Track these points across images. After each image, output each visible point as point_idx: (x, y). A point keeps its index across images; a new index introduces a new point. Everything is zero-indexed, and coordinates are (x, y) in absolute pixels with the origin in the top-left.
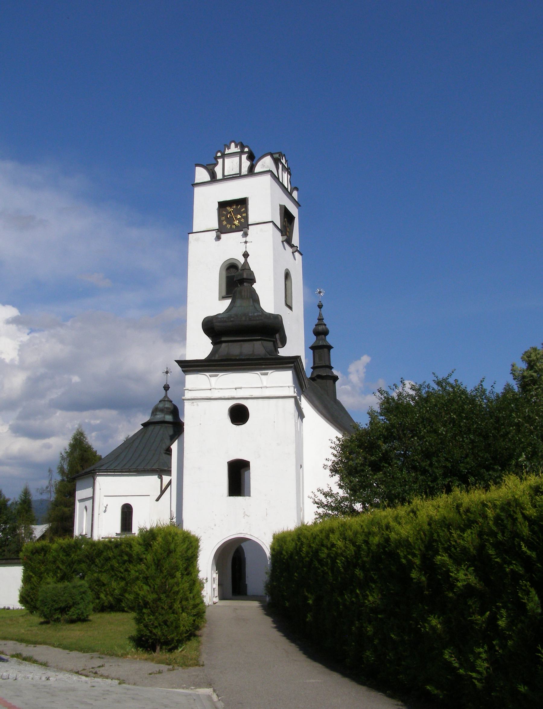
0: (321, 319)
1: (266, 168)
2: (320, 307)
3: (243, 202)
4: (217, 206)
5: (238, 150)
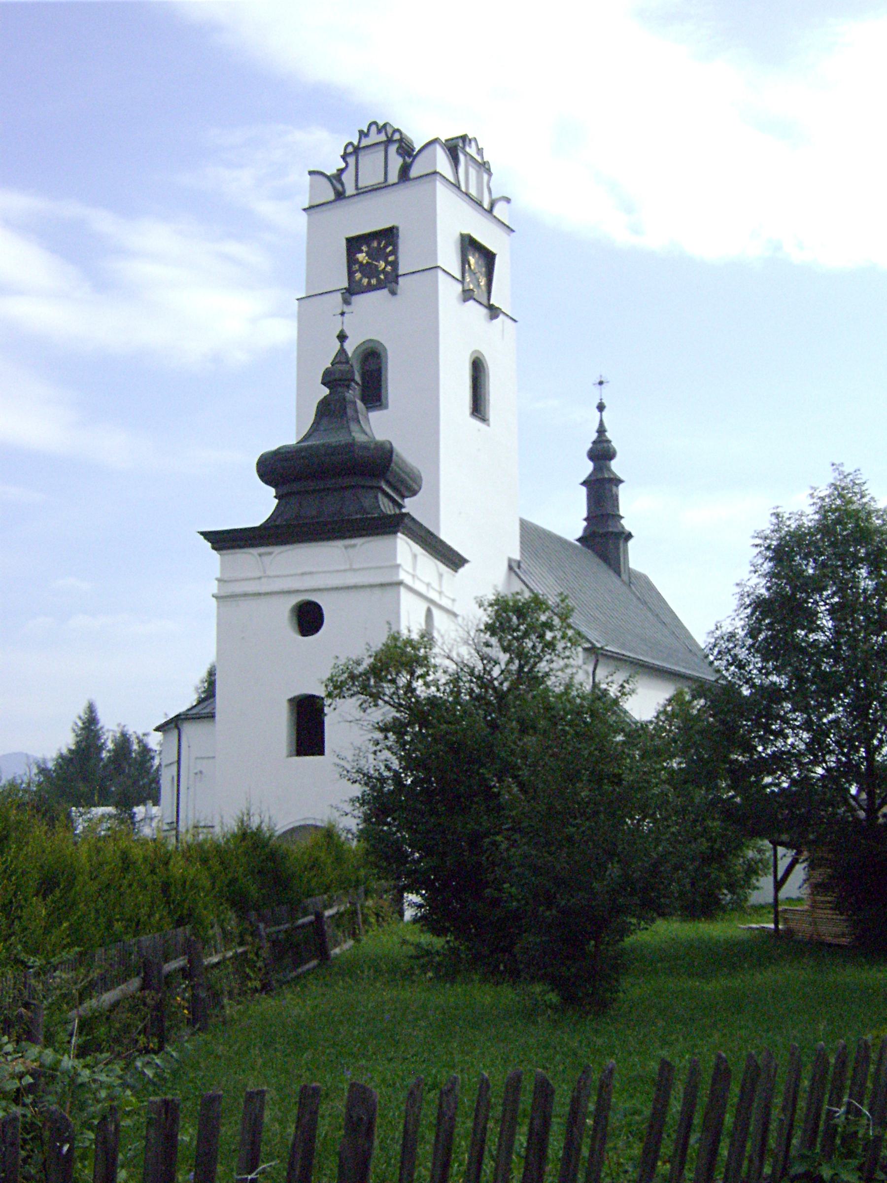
0: (601, 430)
2: (601, 407)
3: (389, 235)
4: (344, 242)
5: (382, 137)
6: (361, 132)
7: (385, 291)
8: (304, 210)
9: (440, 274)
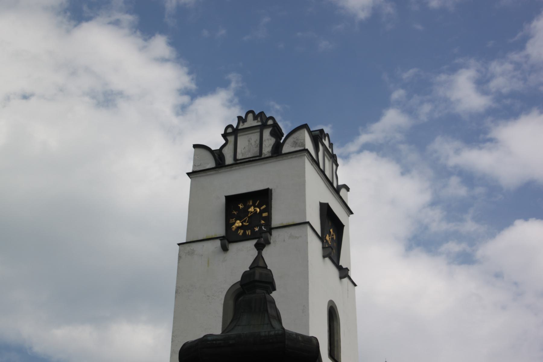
1: (299, 146)
3: (264, 197)
4: (223, 200)
6: (240, 118)
8: (188, 174)
9: (309, 228)
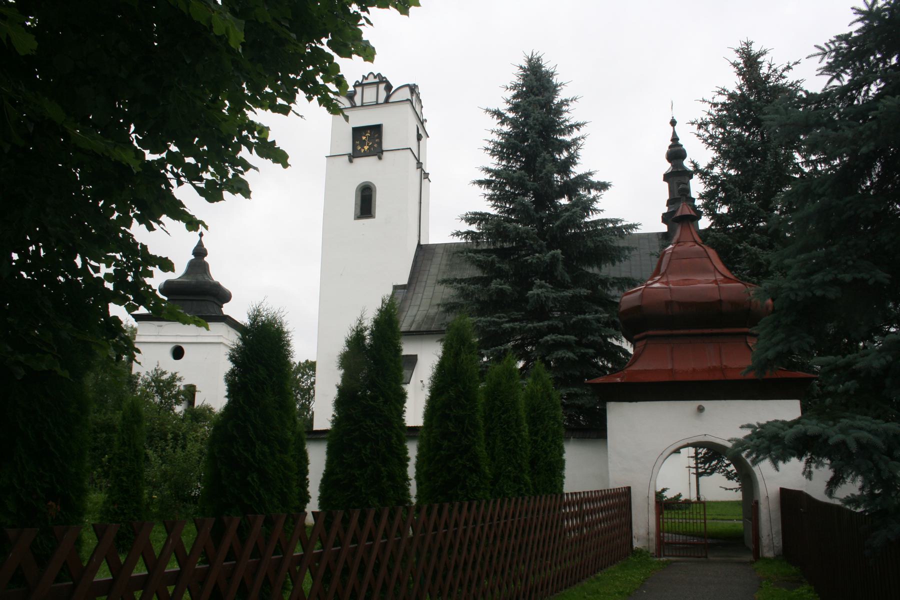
6: (364, 76)
7: (376, 157)
